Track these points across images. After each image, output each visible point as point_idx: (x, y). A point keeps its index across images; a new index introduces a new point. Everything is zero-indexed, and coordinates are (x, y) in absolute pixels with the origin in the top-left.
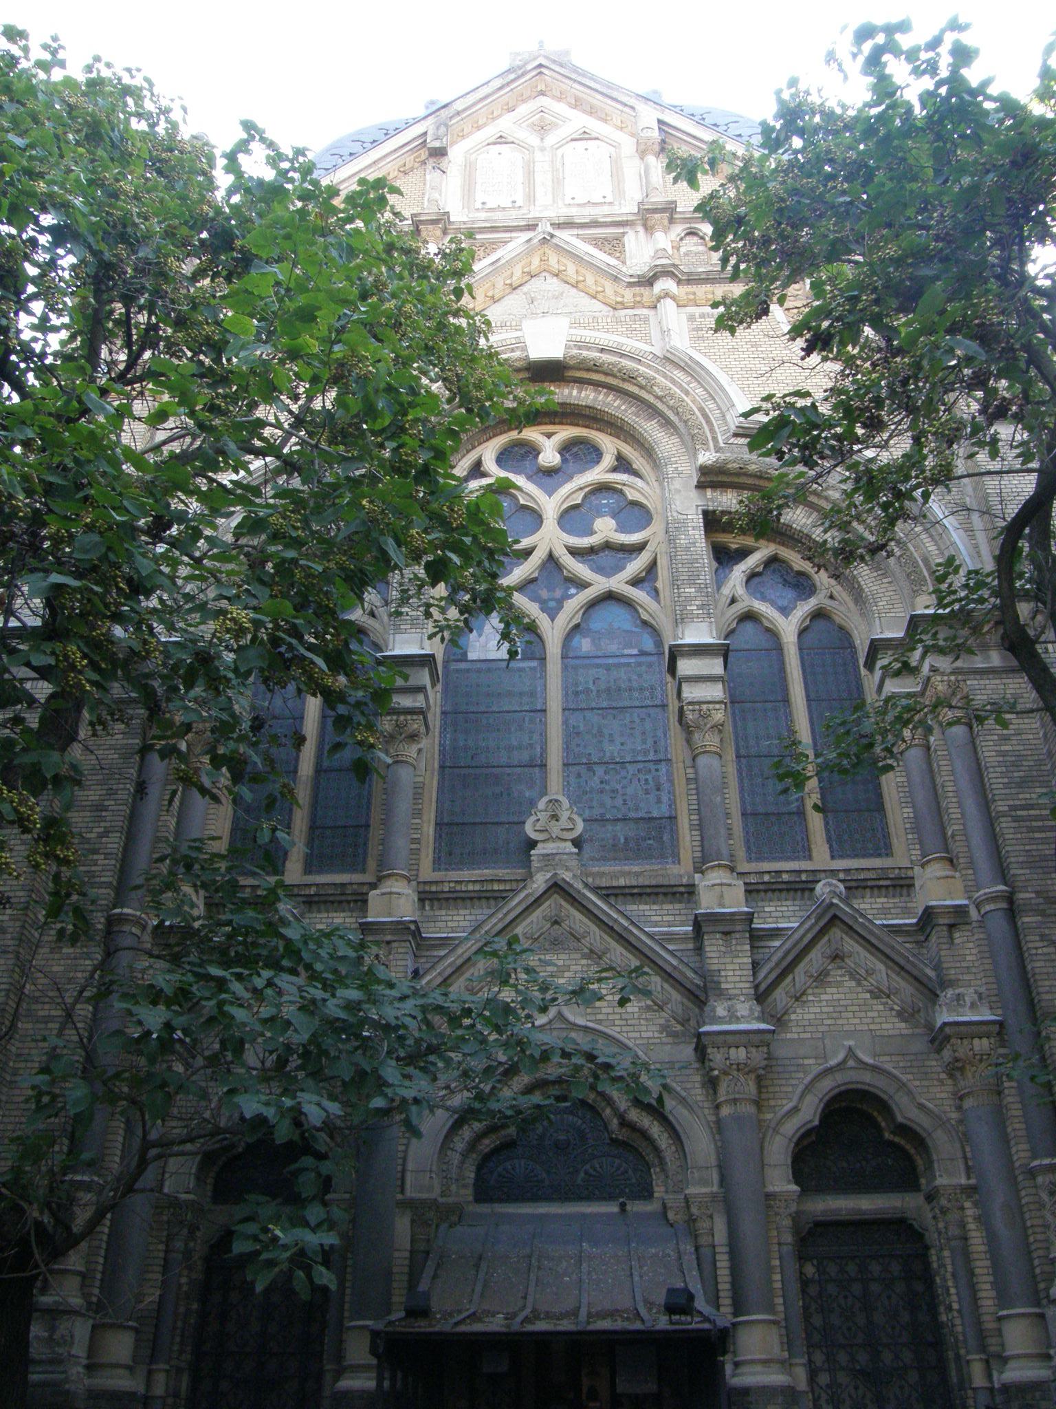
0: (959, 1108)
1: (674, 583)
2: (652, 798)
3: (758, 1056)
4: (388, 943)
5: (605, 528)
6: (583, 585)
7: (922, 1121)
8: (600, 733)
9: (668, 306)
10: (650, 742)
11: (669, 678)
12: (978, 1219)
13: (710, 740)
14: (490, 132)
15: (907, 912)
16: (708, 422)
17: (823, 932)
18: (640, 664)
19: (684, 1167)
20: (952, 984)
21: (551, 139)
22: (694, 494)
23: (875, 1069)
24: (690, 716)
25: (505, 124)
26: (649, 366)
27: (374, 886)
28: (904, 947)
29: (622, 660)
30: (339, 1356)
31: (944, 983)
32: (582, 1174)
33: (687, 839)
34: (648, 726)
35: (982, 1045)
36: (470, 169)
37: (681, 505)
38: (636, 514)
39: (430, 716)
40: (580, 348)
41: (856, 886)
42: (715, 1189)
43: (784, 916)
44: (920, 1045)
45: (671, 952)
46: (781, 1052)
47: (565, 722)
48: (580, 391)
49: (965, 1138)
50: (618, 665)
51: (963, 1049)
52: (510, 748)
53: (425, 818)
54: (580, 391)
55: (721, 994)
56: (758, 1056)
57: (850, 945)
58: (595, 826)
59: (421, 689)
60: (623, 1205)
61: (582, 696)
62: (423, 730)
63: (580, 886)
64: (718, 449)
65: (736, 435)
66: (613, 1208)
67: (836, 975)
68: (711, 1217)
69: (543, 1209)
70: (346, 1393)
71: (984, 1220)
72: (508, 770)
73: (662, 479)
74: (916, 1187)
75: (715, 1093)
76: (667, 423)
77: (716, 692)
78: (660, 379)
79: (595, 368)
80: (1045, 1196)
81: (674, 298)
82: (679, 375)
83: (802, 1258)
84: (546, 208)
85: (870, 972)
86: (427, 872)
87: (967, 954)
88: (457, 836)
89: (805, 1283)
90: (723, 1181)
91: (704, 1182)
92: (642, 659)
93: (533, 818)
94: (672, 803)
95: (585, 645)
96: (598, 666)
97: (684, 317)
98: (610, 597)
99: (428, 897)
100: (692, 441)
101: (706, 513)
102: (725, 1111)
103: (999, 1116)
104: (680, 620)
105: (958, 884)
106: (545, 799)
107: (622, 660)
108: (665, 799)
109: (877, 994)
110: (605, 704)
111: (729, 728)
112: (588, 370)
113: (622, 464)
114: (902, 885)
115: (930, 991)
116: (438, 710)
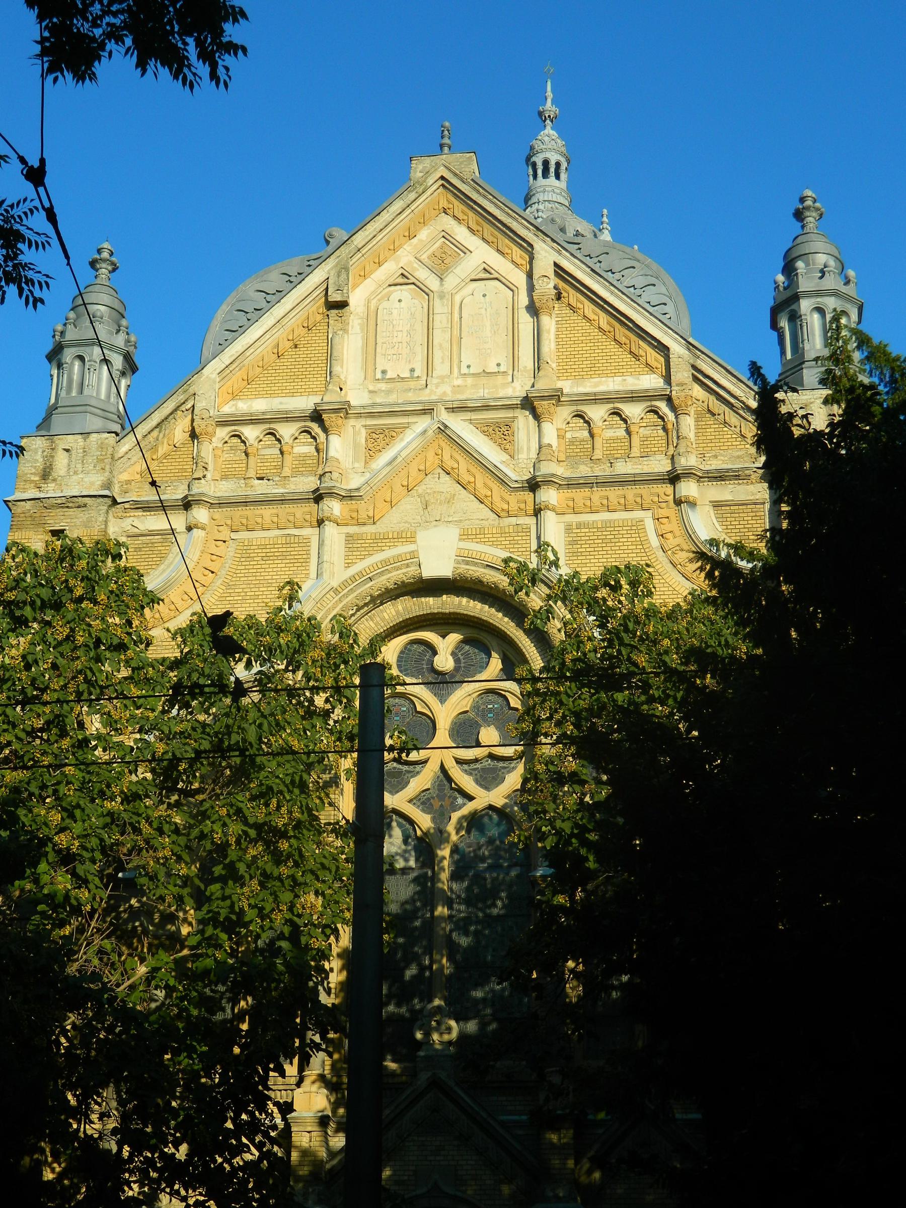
14: (389, 269)
21: (451, 281)
25: (405, 257)
36: (372, 320)
40: (467, 563)
84: (441, 390)
97: (562, 526)
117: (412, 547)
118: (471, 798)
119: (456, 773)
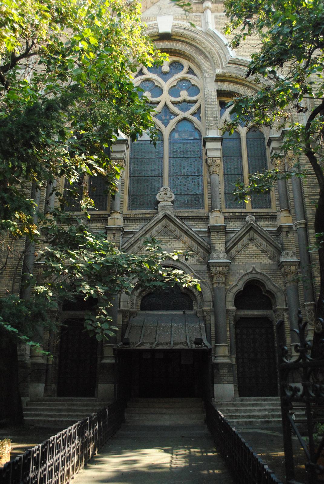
0: (285, 286)
1: (206, 115)
2: (196, 187)
3: (225, 270)
4: (114, 234)
5: (184, 95)
6: (176, 115)
7: (274, 289)
8: (181, 166)
9: (209, 12)
10: (196, 169)
11: (203, 148)
12: (287, 318)
13: (216, 170)
15: (274, 226)
16: (220, 58)
17: (247, 232)
18: (194, 143)
19: (202, 301)
20: (286, 249)
22: (214, 83)
23: (261, 274)
24: (209, 162)
26: (201, 36)
27: (109, 215)
28: (272, 237)
29: (189, 141)
30: (102, 353)
31: (283, 249)
32: (172, 302)
33: (207, 201)
34: (196, 163)
35: (293, 268)
37: (210, 88)
38: (194, 89)
39: (126, 160)
40: (177, 28)
41: (259, 218)
42: (211, 308)
43: (235, 226)
44: (275, 267)
45: (200, 237)
46: (232, 268)
47: (170, 162)
48: (176, 44)
49: (286, 295)
50: (187, 143)
51: (287, 269)
52: (151, 170)
53: (125, 193)
54: (176, 44)
55: (215, 250)
56: (225, 270)
57: (256, 236)
58: (178, 196)
59: (123, 151)
60: (184, 312)
61: (175, 153)
62: (124, 165)
63: (173, 216)
64: (223, 68)
65: (229, 63)
66: (182, 313)
67: (251, 245)
68: (210, 316)
69: (161, 312)
70: (105, 364)
71: (289, 319)
72: (151, 178)
73: (203, 77)
74: (271, 309)
75: (212, 279)
76: (206, 57)
77: (218, 154)
78: (204, 41)
79: (182, 35)
80: (307, 313)
81: (210, 9)
82: (211, 39)
83: (236, 327)
85: (261, 244)
86: (126, 211)
87: (291, 241)
88: (135, 200)
89: (236, 335)
90: (213, 306)
91: (208, 306)
92: (195, 141)
93: (159, 194)
94: (203, 190)
95: (176, 136)
96: (181, 143)
97: (213, 17)
98: (185, 119)
99: (126, 219)
100: (214, 65)
101: (217, 91)
102: (215, 286)
103: (297, 289)
104: (207, 129)
105: (290, 219)
106: (163, 188)
107: (189, 141)
108: (201, 188)
109: (263, 251)
110: (182, 156)
111: (222, 165)
112: (179, 36)
113: (190, 71)
114: (273, 218)
115: (279, 251)
116: (129, 157)
117: (155, 22)
118: (176, 115)
119: (171, 106)
